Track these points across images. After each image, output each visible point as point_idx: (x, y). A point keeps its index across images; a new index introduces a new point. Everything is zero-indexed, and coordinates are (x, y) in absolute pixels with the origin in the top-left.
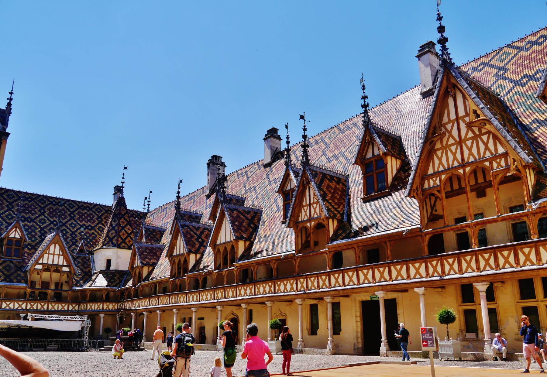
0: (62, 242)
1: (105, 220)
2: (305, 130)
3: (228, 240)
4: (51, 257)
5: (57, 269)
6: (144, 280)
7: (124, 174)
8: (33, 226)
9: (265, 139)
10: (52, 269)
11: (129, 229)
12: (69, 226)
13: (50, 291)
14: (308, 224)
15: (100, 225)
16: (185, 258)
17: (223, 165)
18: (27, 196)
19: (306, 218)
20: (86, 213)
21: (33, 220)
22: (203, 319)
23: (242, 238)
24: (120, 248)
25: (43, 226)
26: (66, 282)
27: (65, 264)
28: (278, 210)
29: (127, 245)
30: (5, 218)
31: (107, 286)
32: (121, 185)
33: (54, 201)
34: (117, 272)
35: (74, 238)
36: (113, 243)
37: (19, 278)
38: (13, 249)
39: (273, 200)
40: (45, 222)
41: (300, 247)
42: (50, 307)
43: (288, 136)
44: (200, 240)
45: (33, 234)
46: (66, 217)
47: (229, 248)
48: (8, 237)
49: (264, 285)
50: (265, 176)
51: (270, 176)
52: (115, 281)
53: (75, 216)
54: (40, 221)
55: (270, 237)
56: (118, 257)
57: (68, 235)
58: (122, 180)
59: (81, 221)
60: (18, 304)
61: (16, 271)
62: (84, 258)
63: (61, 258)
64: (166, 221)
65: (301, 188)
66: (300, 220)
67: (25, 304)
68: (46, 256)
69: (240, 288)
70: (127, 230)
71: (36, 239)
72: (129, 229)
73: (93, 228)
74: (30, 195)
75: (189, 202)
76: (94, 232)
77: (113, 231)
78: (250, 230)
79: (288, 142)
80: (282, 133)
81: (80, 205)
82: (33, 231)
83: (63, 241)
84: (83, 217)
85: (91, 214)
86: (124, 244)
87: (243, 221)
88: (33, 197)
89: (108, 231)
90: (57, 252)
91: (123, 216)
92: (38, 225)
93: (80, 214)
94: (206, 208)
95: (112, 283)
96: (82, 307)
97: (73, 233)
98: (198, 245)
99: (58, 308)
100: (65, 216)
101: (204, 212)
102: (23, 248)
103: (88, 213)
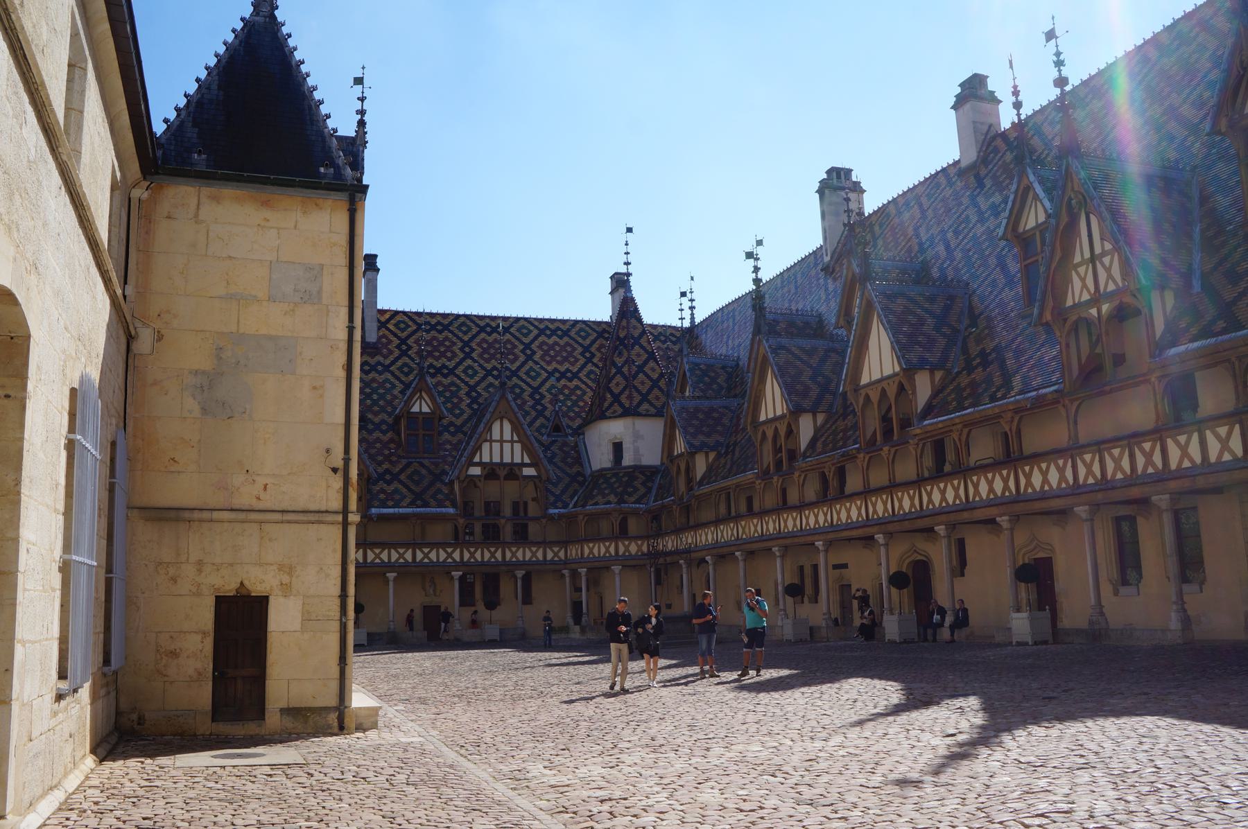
0: (515, 414)
1: (598, 355)
2: (1059, 64)
3: (888, 371)
4: (496, 446)
5: (512, 471)
6: (701, 483)
8: (453, 384)
9: (955, 107)
11: (653, 370)
13: (503, 521)
14: (1094, 312)
15: (589, 367)
16: (789, 425)
17: (857, 188)
18: (433, 321)
19: (1086, 297)
20: (556, 343)
21: (452, 372)
22: (845, 566)
23: (922, 365)
24: (639, 415)
25: (472, 382)
26: (533, 500)
27: (527, 460)
28: (1010, 283)
29: (655, 407)
30: (397, 373)
32: (623, 269)
33: (488, 325)
34: (638, 469)
35: (538, 402)
36: (621, 405)
37: (440, 496)
39: (993, 261)
40: (476, 373)
41: (1075, 372)
42: (508, 555)
43: (1015, 87)
44: (820, 379)
45: (455, 401)
46: (516, 358)
47: (892, 392)
48: (409, 412)
49: (990, 476)
50: (965, 201)
51: (981, 200)
52: (636, 490)
53: (534, 353)
54: (465, 371)
55: (994, 355)
56: (637, 436)
57: (526, 396)
59: (549, 363)
61: (432, 484)
62: (565, 444)
63: (518, 447)
64: (736, 343)
65: (1065, 219)
66: (1069, 303)
67: (458, 551)
68: (486, 446)
69: (929, 488)
70: (649, 372)
71: (463, 412)
72: (653, 370)
73: (575, 375)
74: (439, 318)
75: (786, 289)
76: (579, 383)
77: (619, 378)
78: (942, 342)
79: (1018, 105)
80: (999, 85)
81: (542, 326)
82: (454, 394)
83: (516, 409)
84: (552, 353)
85: (567, 344)
86: (645, 406)
87: (922, 322)
88: (446, 322)
90: (507, 436)
92: (463, 381)
93: (545, 348)
94: (827, 300)
95: (630, 495)
96: (574, 551)
97: (536, 390)
98: (815, 392)
100: (514, 354)
101: (823, 309)
102: (440, 434)
103: (562, 342)
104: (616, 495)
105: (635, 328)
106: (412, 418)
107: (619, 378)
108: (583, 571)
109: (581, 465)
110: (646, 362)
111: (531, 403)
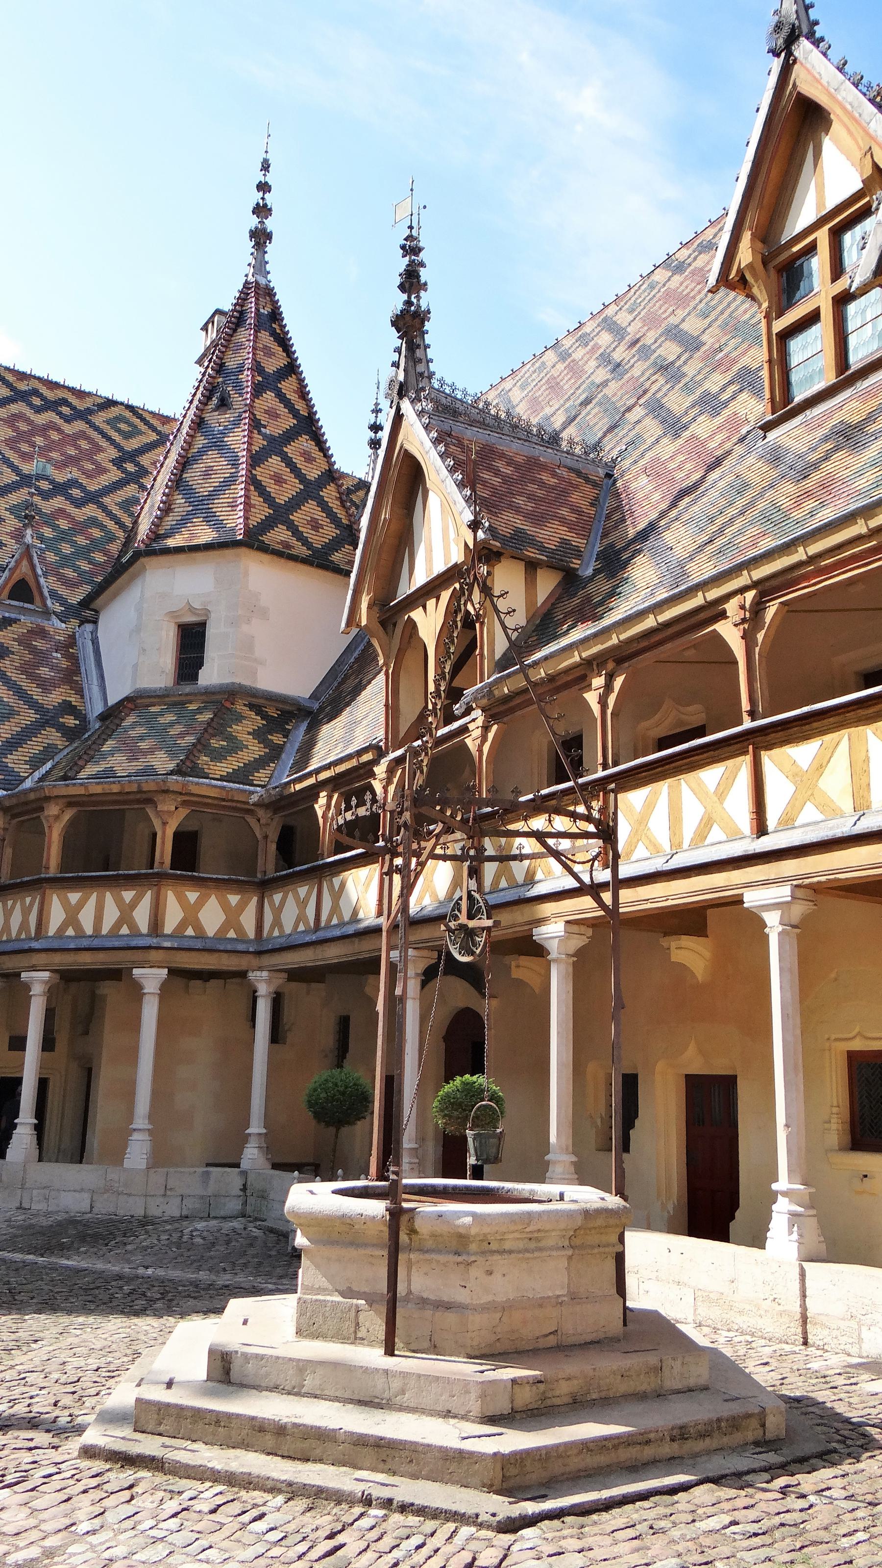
7: (266, 166)
15: (131, 490)
20: (52, 426)
24: (264, 549)
31: (178, 771)
52: (235, 746)
62: (41, 633)
70: (299, 461)
73: (93, 498)
76: (100, 515)
81: (23, 386)
84: (39, 441)
85: (82, 435)
86: (279, 535)
89: (185, 463)
93: (23, 427)
95: (218, 756)
104: (172, 754)
105: (268, 352)
107: (212, 459)
109: (80, 692)
110: (290, 436)
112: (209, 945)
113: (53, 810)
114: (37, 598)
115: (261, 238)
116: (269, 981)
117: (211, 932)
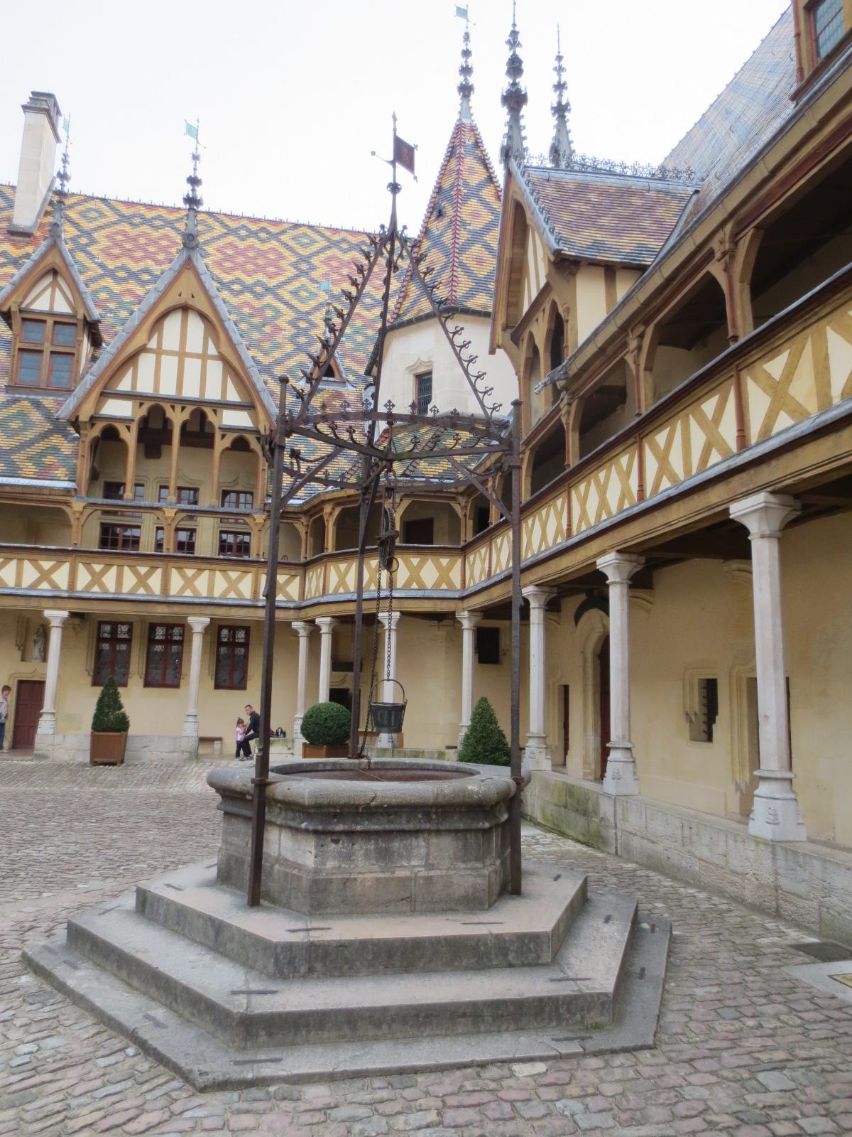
0: (210, 299)
4: (170, 364)
7: (467, 37)
10: (178, 418)
12: (287, 297)
27: (233, 396)
37: (49, 460)
38: (47, 354)
46: (281, 271)
53: (313, 268)
57: (282, 322)
58: (461, 61)
60: (39, 568)
61: (45, 436)
63: (215, 368)
68: (146, 361)
81: (337, 238)
88: (172, 217)
91: (474, 192)
93: (334, 263)
99: (211, 587)
105: (472, 171)
106: (36, 320)
108: (324, 623)
111: (290, 331)
112: (427, 594)
113: (328, 509)
114: (336, 373)
115: (466, 90)
116: (469, 618)
117: (429, 586)
